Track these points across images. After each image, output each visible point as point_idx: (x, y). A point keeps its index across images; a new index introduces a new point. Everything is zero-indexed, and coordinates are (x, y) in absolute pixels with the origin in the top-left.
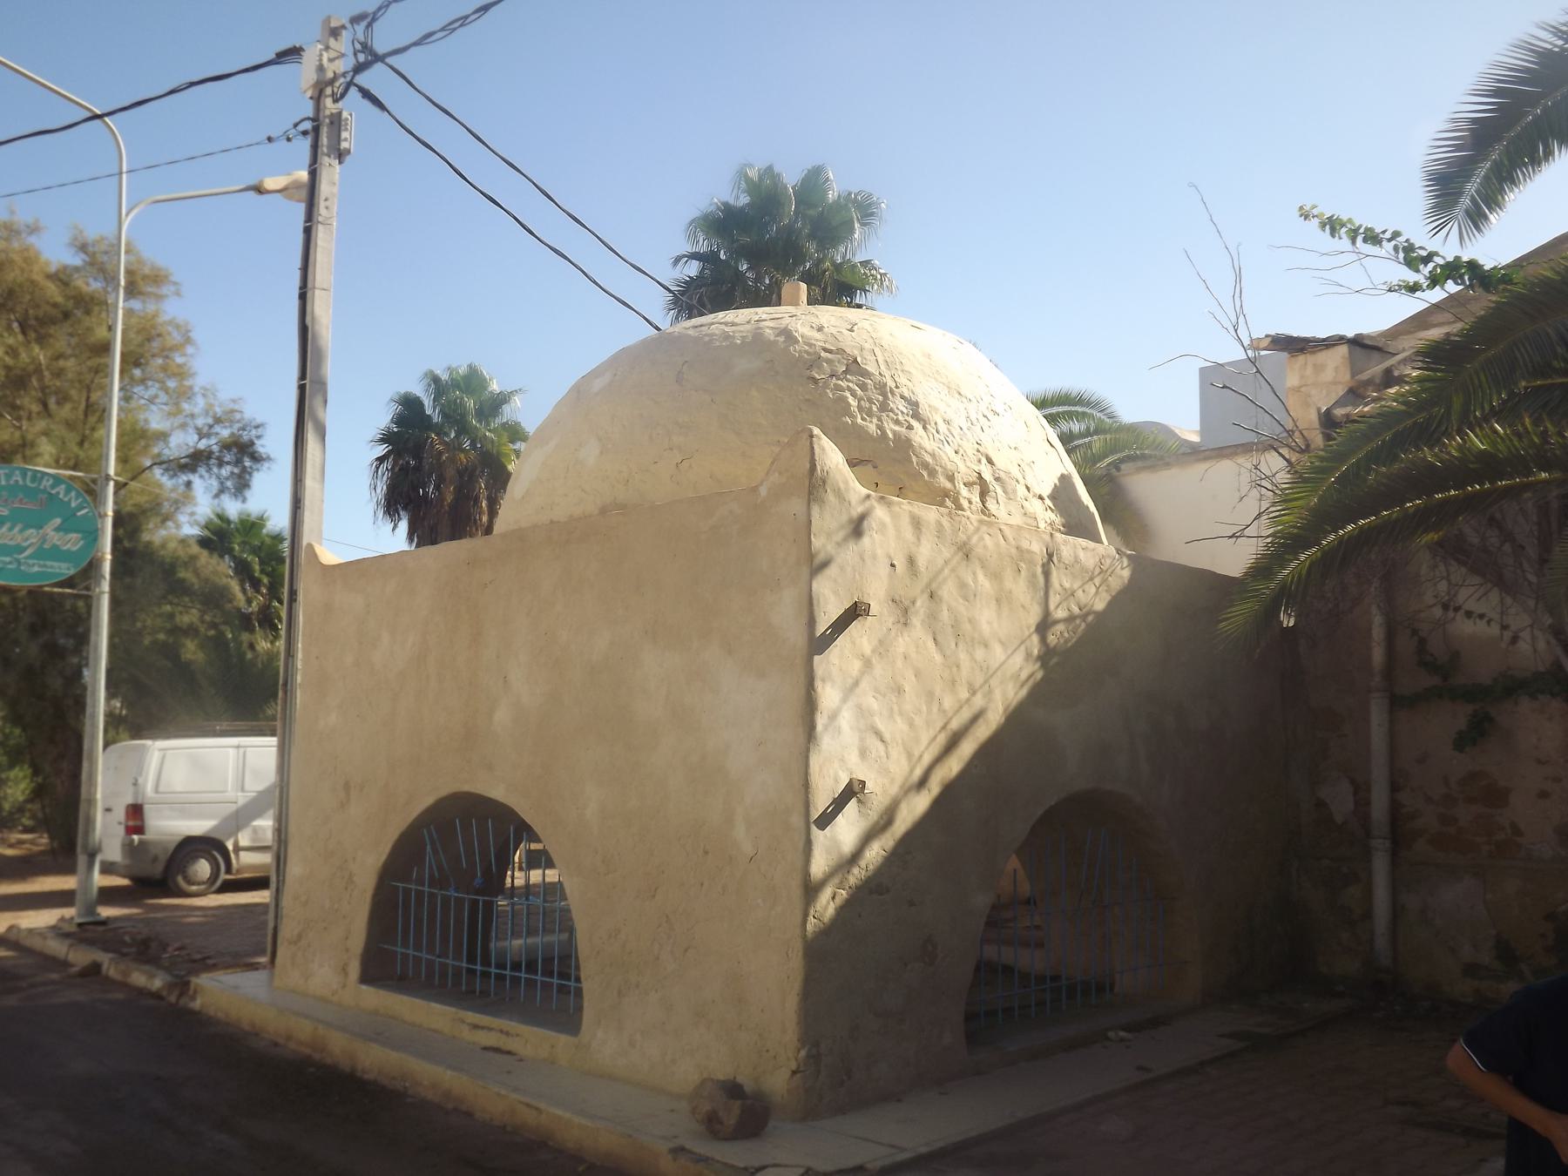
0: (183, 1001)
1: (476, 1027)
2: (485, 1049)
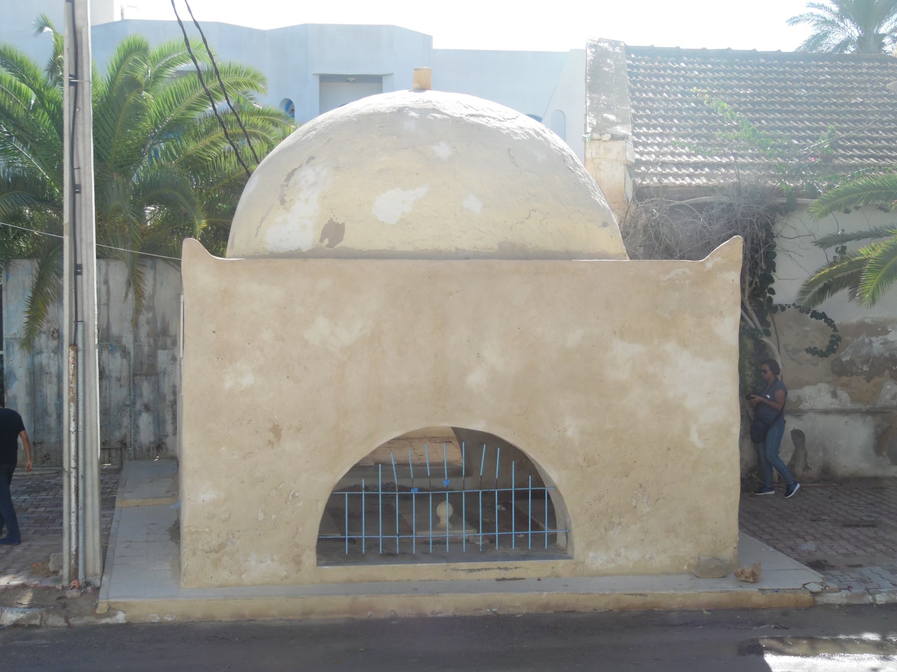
0: (76, 622)
1: (470, 571)
2: (498, 580)
